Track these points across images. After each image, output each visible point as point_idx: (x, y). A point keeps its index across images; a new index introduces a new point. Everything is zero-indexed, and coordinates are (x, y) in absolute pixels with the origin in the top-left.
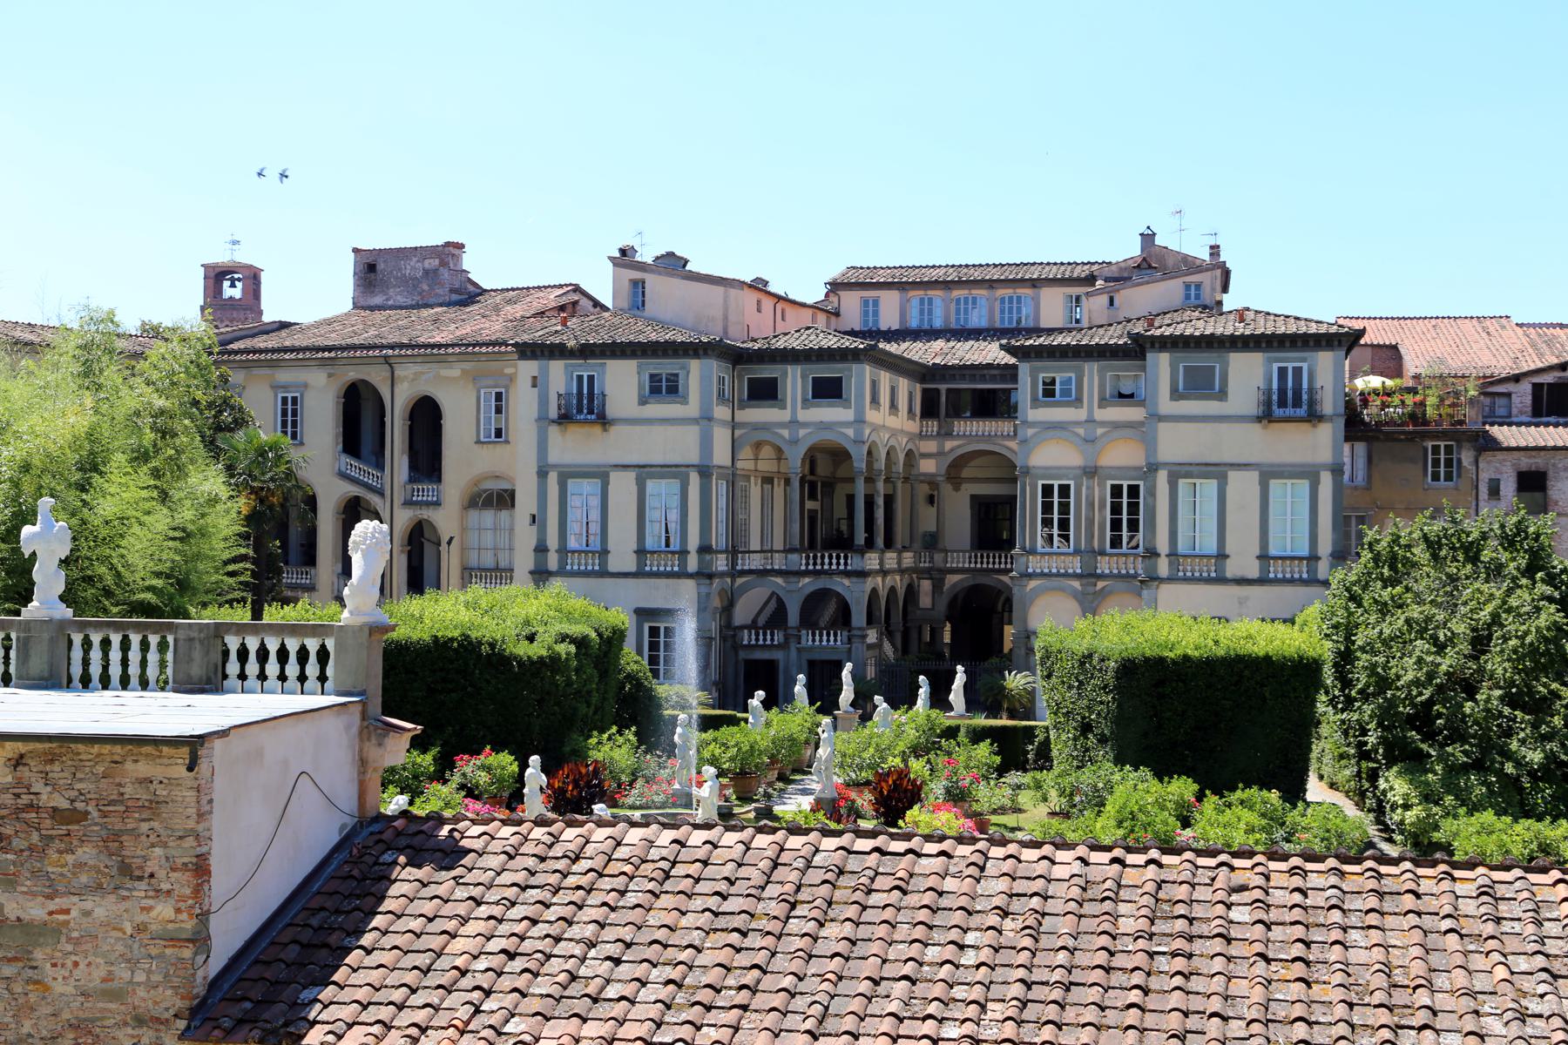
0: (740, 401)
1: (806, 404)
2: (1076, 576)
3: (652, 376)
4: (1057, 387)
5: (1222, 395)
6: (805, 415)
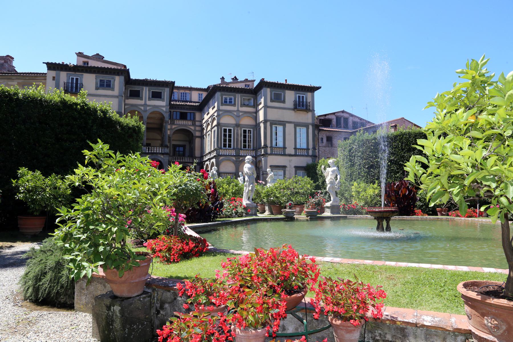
0: (127, 96)
1: (149, 99)
2: (234, 156)
3: (101, 81)
4: (228, 101)
5: (284, 102)
6: (149, 103)
